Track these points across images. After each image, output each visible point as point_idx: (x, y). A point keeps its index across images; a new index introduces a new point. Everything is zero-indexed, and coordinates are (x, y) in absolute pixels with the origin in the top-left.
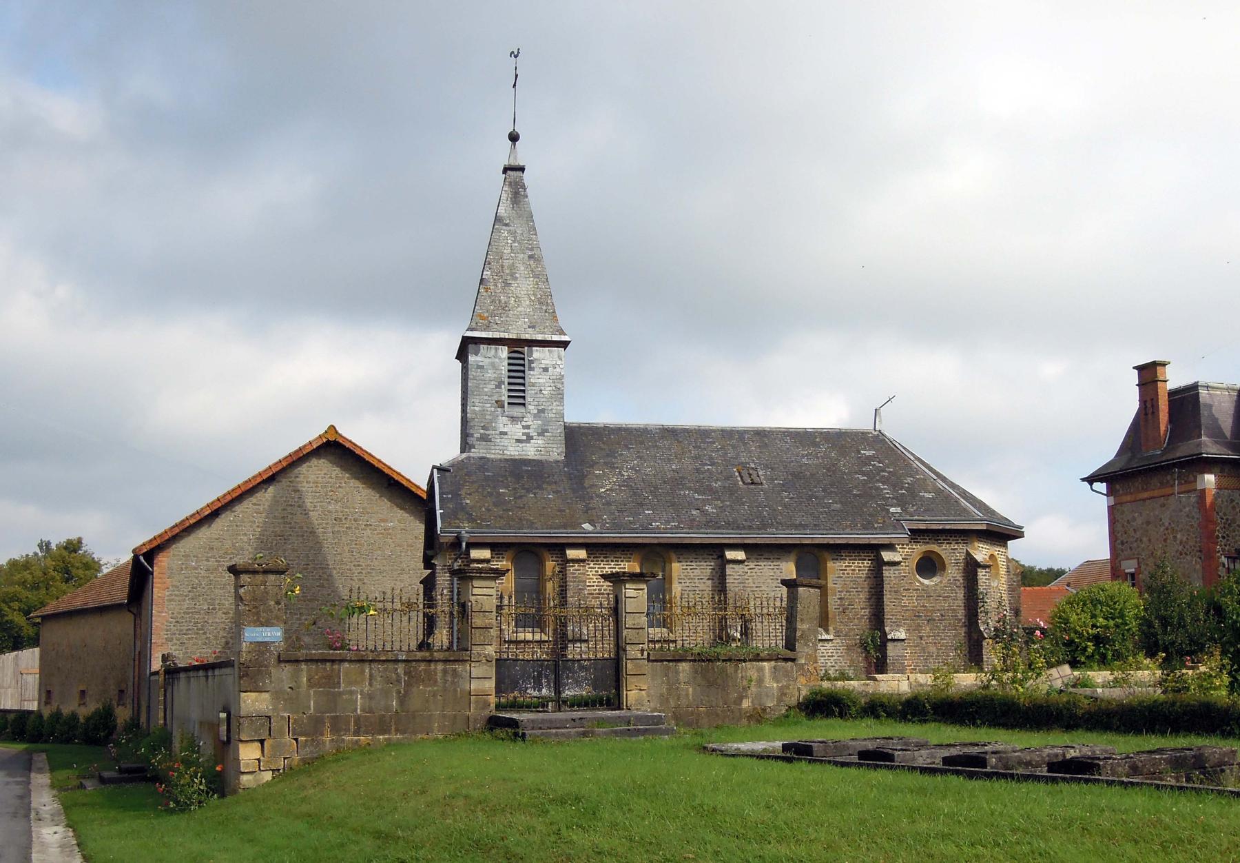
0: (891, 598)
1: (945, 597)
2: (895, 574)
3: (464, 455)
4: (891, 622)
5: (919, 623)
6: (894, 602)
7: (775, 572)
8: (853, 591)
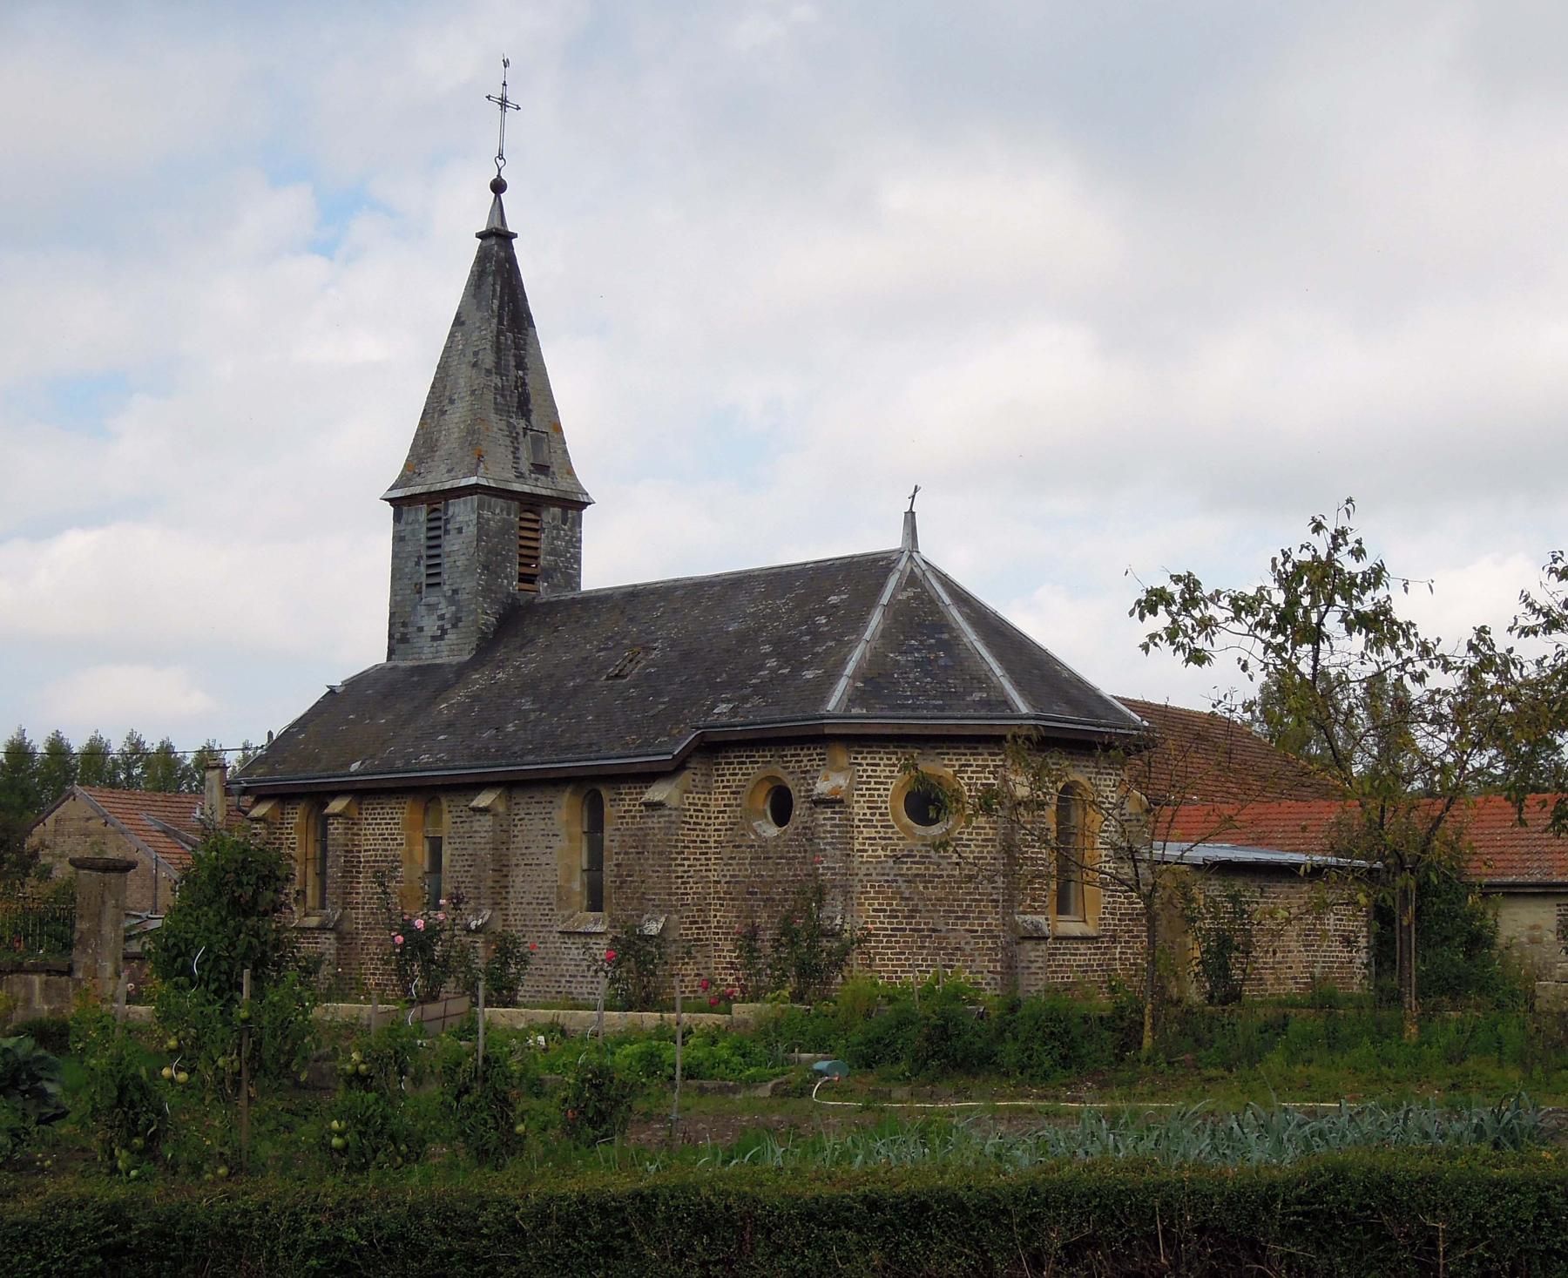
0: (654, 866)
1: (790, 858)
2: (659, 822)
3: (391, 664)
4: (653, 905)
5: (752, 906)
6: (658, 871)
7: (546, 824)
8: (632, 853)
